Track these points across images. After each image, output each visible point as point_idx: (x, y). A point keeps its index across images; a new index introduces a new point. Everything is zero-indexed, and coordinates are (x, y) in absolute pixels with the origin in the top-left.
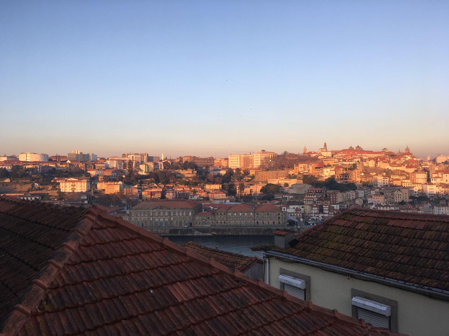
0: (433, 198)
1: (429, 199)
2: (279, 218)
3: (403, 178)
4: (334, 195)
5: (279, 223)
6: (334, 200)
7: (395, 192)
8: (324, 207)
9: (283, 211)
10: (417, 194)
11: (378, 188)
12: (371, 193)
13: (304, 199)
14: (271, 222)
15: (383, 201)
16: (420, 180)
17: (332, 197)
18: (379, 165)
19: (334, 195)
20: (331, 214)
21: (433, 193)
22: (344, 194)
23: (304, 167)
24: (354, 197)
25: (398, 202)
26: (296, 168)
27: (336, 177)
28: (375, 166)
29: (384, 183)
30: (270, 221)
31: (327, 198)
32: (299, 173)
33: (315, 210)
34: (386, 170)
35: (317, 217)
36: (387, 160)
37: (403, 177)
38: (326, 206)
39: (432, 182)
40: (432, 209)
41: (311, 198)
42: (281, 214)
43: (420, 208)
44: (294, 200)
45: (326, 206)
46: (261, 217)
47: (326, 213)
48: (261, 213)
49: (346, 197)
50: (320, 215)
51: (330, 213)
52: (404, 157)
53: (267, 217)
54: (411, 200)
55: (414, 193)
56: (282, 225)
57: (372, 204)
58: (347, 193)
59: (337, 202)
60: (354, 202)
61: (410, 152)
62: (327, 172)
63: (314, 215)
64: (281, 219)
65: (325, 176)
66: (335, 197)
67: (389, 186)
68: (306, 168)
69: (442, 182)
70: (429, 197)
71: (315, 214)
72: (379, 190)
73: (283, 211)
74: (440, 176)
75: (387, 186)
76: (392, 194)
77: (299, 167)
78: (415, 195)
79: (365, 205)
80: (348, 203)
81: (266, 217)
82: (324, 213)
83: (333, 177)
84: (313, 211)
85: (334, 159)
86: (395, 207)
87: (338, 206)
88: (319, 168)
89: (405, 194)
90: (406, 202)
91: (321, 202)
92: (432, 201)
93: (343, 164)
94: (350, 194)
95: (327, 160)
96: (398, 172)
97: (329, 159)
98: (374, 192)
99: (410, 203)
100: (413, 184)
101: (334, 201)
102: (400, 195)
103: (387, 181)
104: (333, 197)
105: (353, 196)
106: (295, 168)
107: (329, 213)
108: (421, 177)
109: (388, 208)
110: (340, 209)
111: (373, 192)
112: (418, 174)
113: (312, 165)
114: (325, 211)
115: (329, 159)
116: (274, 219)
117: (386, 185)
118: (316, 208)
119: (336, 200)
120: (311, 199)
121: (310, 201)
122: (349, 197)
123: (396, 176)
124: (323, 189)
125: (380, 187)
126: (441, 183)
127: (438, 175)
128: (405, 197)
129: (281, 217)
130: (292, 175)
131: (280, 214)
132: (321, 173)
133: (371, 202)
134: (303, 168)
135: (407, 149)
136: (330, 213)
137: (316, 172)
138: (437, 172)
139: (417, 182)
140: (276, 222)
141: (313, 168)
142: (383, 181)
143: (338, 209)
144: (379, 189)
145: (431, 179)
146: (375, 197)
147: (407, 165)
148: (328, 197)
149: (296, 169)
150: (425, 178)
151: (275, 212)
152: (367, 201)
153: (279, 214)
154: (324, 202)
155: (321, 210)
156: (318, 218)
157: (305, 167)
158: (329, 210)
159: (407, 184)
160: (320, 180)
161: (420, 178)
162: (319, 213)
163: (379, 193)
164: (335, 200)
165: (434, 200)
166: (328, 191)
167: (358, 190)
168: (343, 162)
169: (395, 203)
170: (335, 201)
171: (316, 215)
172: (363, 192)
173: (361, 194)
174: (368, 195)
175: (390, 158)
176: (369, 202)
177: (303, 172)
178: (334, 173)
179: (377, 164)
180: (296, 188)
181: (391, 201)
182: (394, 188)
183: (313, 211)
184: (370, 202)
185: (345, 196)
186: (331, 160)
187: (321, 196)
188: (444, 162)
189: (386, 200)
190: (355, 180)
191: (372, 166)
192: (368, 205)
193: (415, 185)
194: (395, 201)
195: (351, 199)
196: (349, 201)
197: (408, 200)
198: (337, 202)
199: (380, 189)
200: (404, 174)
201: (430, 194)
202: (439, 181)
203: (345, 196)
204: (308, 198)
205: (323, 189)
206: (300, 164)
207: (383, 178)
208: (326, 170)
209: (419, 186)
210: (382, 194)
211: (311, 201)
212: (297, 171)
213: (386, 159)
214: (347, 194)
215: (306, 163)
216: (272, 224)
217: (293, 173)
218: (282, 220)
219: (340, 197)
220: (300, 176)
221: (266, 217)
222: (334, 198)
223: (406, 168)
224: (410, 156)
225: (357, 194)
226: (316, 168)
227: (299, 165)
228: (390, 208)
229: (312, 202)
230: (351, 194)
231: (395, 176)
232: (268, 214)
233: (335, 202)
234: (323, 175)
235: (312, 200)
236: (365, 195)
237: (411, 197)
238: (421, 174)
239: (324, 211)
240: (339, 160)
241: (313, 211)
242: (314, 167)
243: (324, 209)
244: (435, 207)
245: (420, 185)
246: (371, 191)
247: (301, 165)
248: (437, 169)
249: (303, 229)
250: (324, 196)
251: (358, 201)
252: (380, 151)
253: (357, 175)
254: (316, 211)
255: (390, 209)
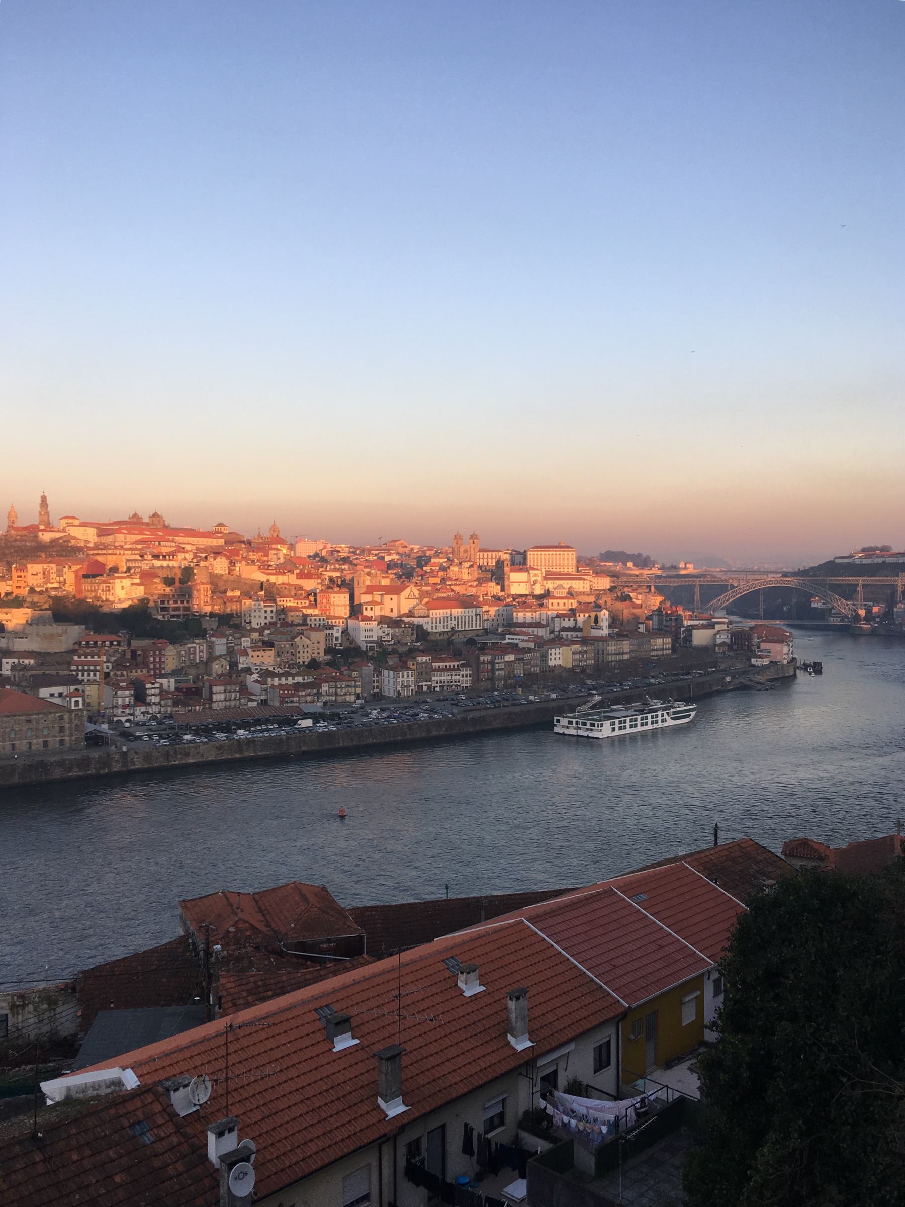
0: (374, 650)
1: (366, 652)
2: (62, 729)
3: (303, 605)
4: (157, 653)
5: (62, 742)
6: (158, 666)
7: (297, 639)
8: (148, 686)
9: (73, 707)
10: (340, 641)
11: (254, 630)
12: (241, 644)
13: (73, 668)
14: (37, 743)
15: (272, 663)
16: (340, 608)
17: (152, 659)
18: (238, 569)
19: (157, 653)
20: (166, 705)
21: (371, 639)
22: (180, 648)
23: (44, 574)
24: (205, 656)
25: (301, 663)
26: (20, 574)
27: (151, 604)
28: (229, 573)
29: (266, 618)
30: (35, 741)
31: (136, 660)
32: (32, 591)
33: (125, 696)
34: (264, 584)
35: (130, 714)
36: (242, 555)
37: (303, 602)
38: (153, 684)
39: (365, 613)
40: (377, 677)
41: (96, 664)
42: (66, 717)
43: (355, 674)
44: (40, 672)
45: (153, 684)
46: (8, 730)
47: (154, 704)
48: (7, 719)
49: (185, 657)
50: (138, 708)
51: (162, 702)
52: (274, 549)
53: (25, 728)
54: (329, 657)
55: (334, 639)
56: (71, 750)
57: (248, 671)
58: (189, 645)
59: (163, 672)
60: (206, 669)
61: (282, 535)
62: (123, 588)
63: (120, 710)
64: (67, 732)
65: (116, 600)
66: (160, 659)
67: (278, 625)
68: (53, 576)
69: (382, 614)
70: (364, 649)
71: (125, 707)
72: (260, 635)
73: (73, 707)
74: (378, 598)
75: (273, 624)
76: (292, 645)
77: (30, 573)
78: (336, 645)
79: (235, 675)
80: (193, 672)
81: (21, 730)
82: (149, 704)
83: (144, 602)
84: (120, 701)
85: (122, 552)
86: (304, 676)
87: (172, 680)
88: (94, 576)
89: (316, 642)
90: (320, 663)
91: (125, 673)
92: (372, 658)
93: (153, 567)
94: (195, 648)
95: (104, 554)
96: (289, 590)
97: (110, 552)
98: (247, 641)
99: (330, 664)
100: (327, 619)
101: (157, 669)
102: (305, 646)
103: (272, 611)
104: (155, 659)
105: (201, 654)
106: (15, 574)
107: (159, 703)
108: (339, 603)
109: (290, 679)
110: (176, 689)
111: (246, 642)
112: (336, 595)
113: (75, 568)
114: (150, 698)
115: (110, 552)
116: (45, 732)
117: (270, 622)
118: (127, 692)
119: (163, 666)
120: (95, 666)
121: (92, 671)
122: (192, 656)
123: (288, 599)
124: (120, 637)
125: (258, 627)
126: (382, 616)
127: (372, 597)
128: (316, 652)
129: (67, 726)
130: (7, 594)
131: (65, 717)
132: (103, 591)
133: (245, 666)
134: (41, 576)
135: (274, 528)
136: (162, 702)
137: (88, 587)
138: (370, 590)
139: (332, 614)
140: (54, 742)
141: (76, 576)
142: (263, 611)
143: (173, 688)
144: (258, 633)
145: (364, 607)
146: (256, 654)
147: (298, 571)
148: (140, 659)
149: (18, 577)
150: (345, 606)
151: (51, 713)
152: (237, 664)
153: (61, 718)
154: (131, 672)
155: (140, 697)
156: (131, 718)
157: (49, 572)
158: (160, 694)
159: (315, 620)
160: (106, 609)
161: (340, 603)
162: (135, 705)
163: (260, 644)
164: (160, 666)
165: (375, 656)
166: (135, 643)
167: (212, 636)
168: (154, 562)
169: (299, 666)
170: (161, 669)
171: (127, 711)
172: (224, 641)
173: (220, 646)
174: (236, 648)
175: (247, 552)
176: (241, 666)
177: (43, 587)
178: (140, 593)
179: (232, 568)
180: (37, 634)
181: (291, 662)
182: (289, 629)
183: (120, 701)
184: (243, 666)
185: (183, 653)
186: (115, 554)
187: (119, 656)
188: (311, 554)
189: (278, 660)
190: (197, 612)
191: (222, 572)
192: (242, 675)
193: (336, 622)
194: (301, 661)
195: (198, 661)
196: (196, 666)
197: (322, 657)
198: (163, 672)
199: (261, 631)
200: (302, 594)
201: (366, 642)
202: (377, 612)
203: (183, 653)
204: (84, 664)
205: (120, 637)
206: (29, 563)
207: (265, 606)
208: (121, 582)
209: (339, 622)
210: (269, 645)
211: (95, 671)
212: (21, 584)
213: (241, 552)
214: (189, 648)
215: (50, 562)
216: (42, 749)
217: (9, 589)
218: (71, 735)
219: (171, 657)
220: (35, 601)
221: (21, 730)
222: (158, 660)
223: (297, 578)
224: (286, 546)
225: (211, 647)
226: (85, 576)
227: (29, 566)
228: (293, 679)
229: (98, 673)
230: (198, 648)
231: (285, 599)
232: (29, 721)
233: (161, 672)
234: (111, 598)
235: (98, 668)
236: (228, 648)
237: (328, 651)
238: (342, 596)
239: (149, 698)
240: (142, 556)
241: (120, 699)
242: (81, 573)
243: (149, 692)
244: (386, 672)
245: (341, 621)
246: (243, 639)
247: (35, 568)
248: (368, 583)
249: (136, 753)
250: (128, 656)
251: (217, 667)
252: (209, 527)
253: (202, 597)
254: (127, 700)
255: (294, 682)
